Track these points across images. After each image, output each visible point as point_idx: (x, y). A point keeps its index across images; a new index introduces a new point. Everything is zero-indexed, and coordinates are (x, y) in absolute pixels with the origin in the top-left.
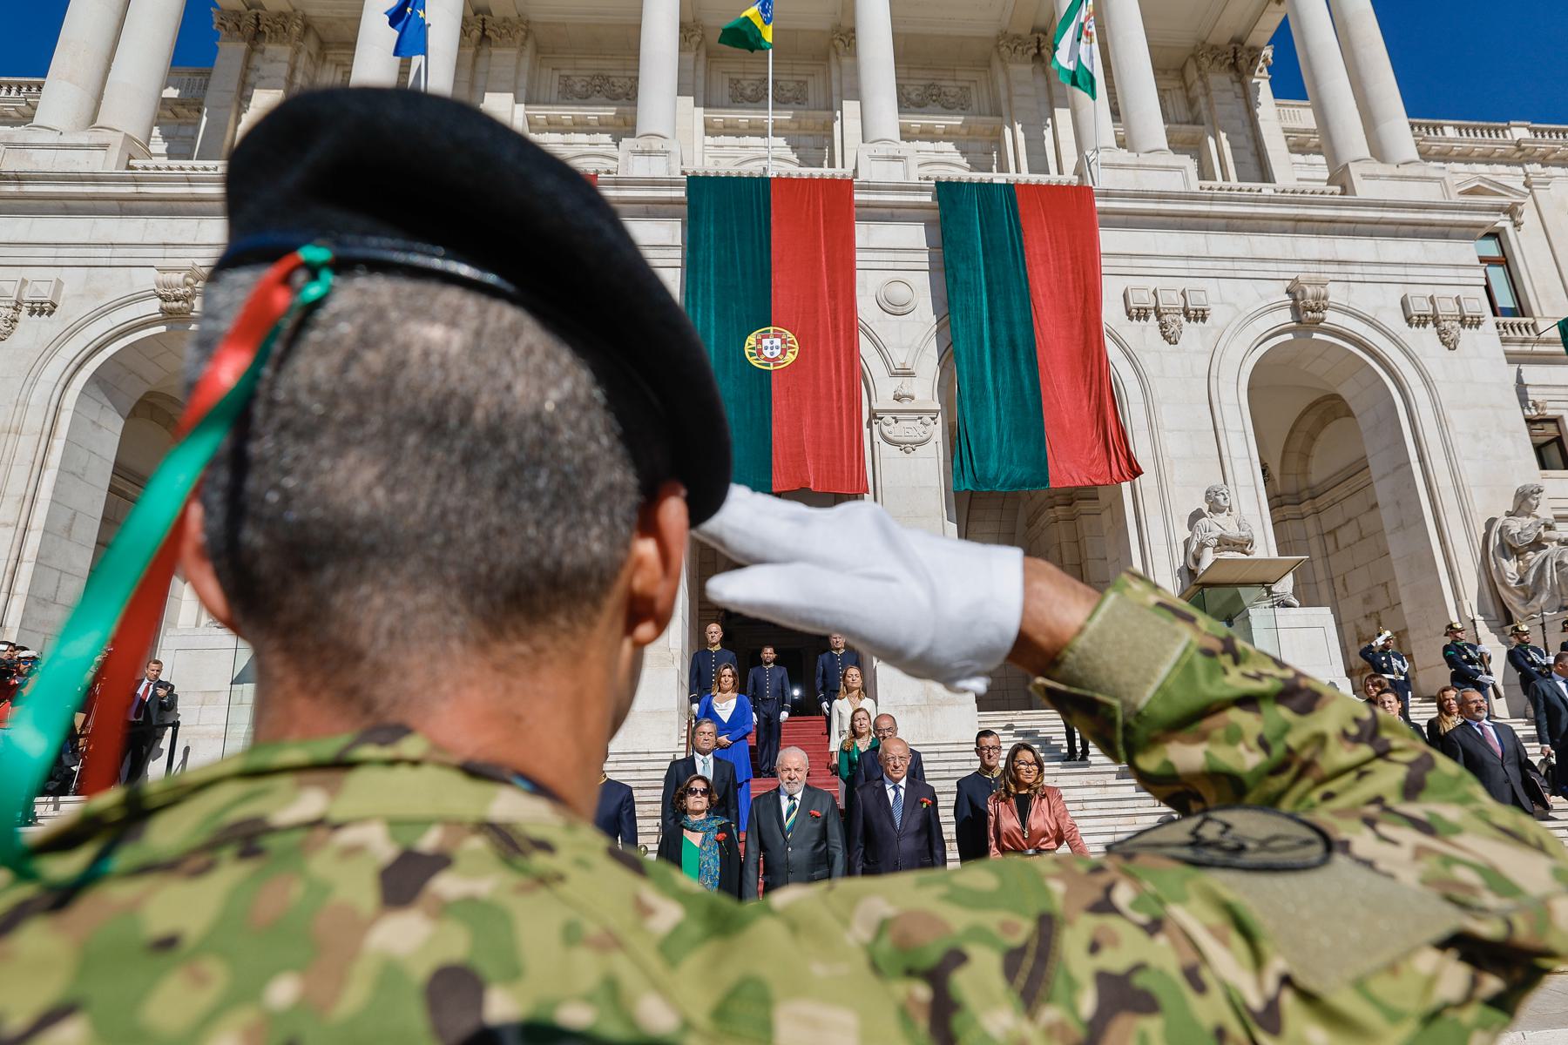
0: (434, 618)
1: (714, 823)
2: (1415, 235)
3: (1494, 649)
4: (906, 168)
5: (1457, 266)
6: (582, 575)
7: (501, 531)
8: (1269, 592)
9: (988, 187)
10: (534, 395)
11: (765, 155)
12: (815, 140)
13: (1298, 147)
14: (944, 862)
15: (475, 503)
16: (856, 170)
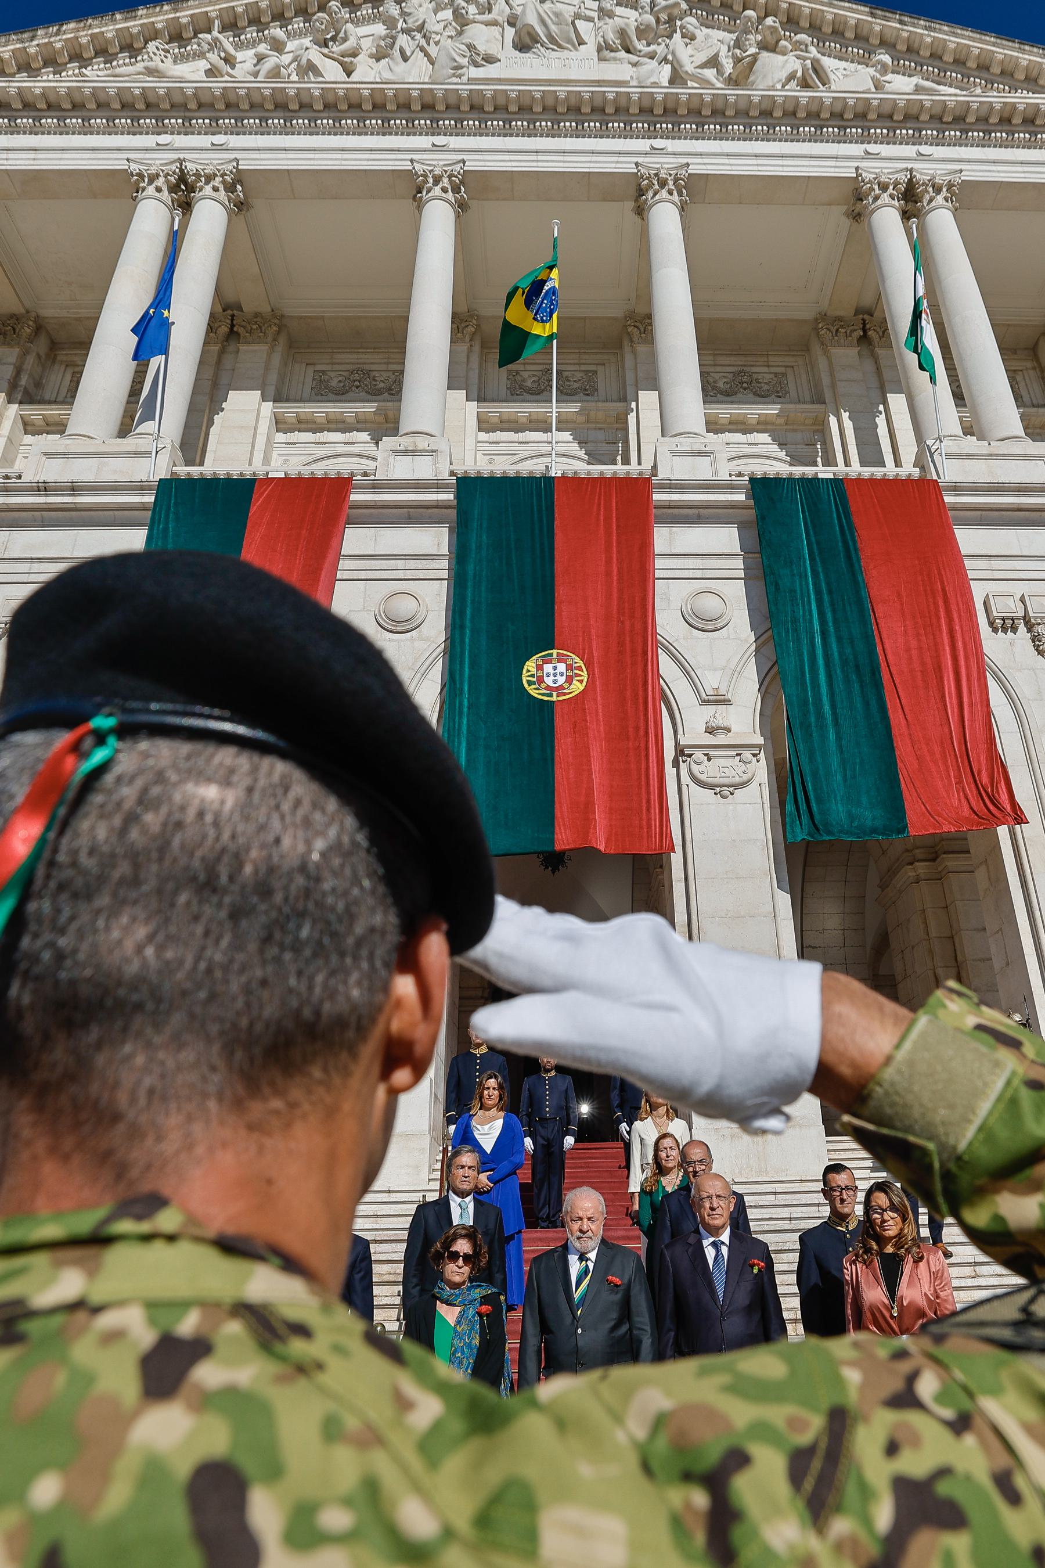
0: (193, 1077)
4: (714, 465)
6: (340, 1023)
7: (264, 983)
9: (811, 484)
10: (301, 848)
12: (607, 435)
15: (240, 957)
16: (655, 467)
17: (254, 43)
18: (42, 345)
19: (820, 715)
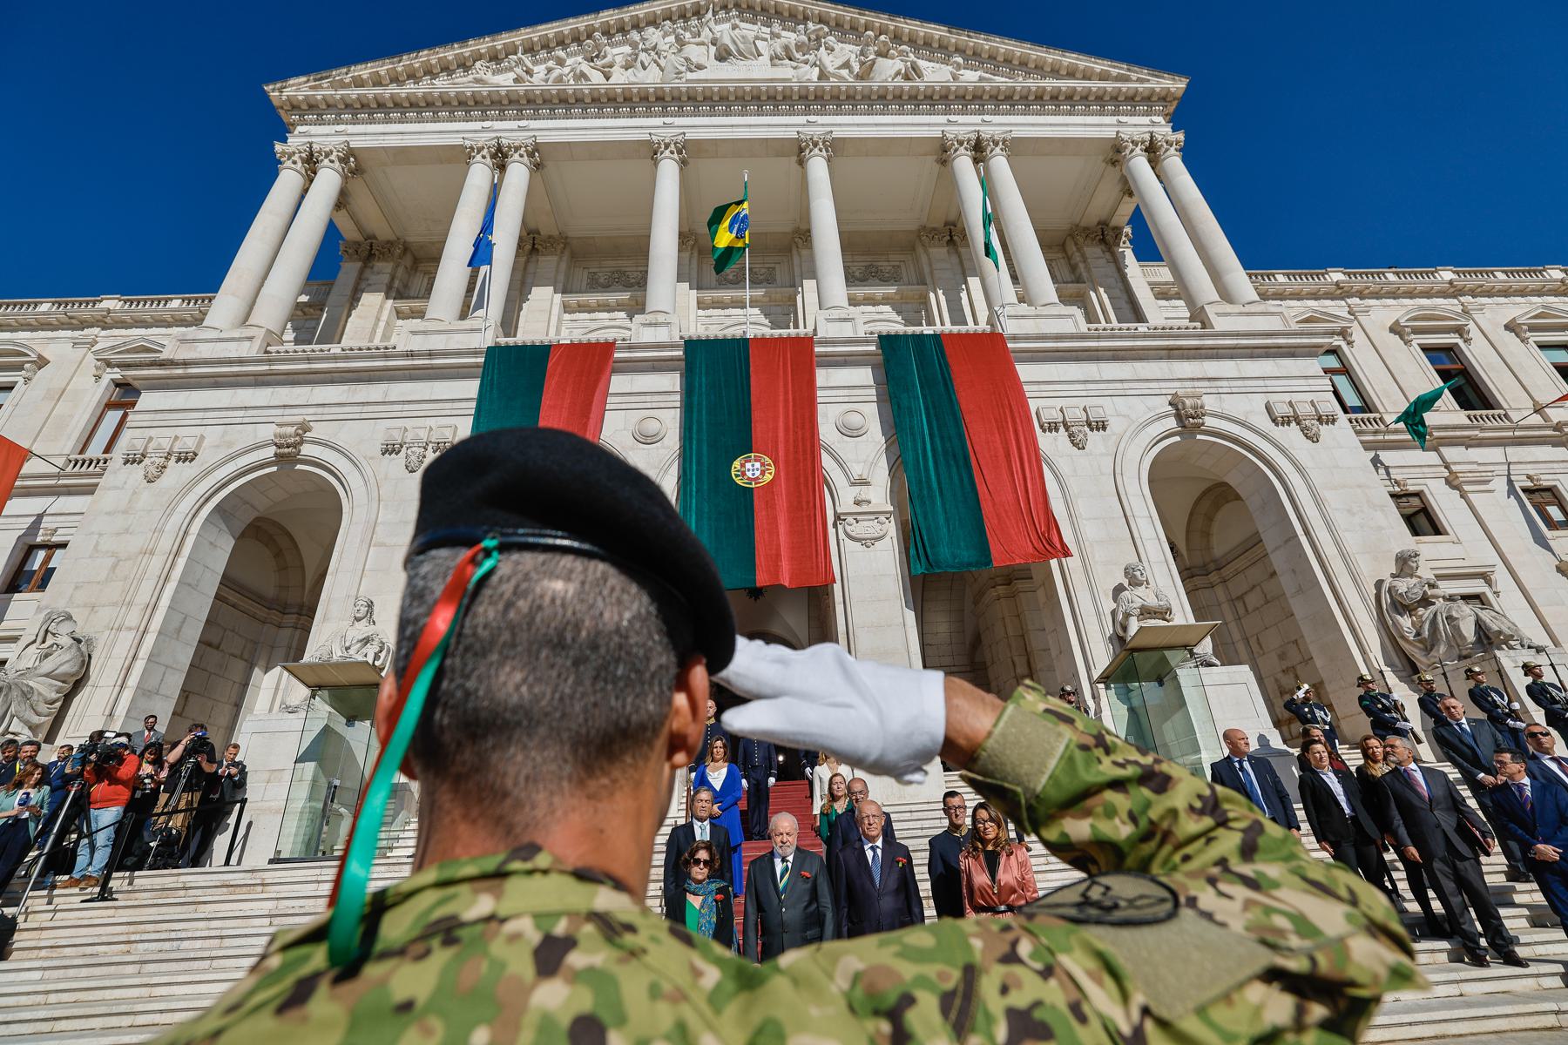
1: (713, 886)
2: (1268, 356)
3: (1405, 696)
5: (1306, 377)
8: (1192, 654)
9: (919, 338)
11: (745, 320)
12: (783, 310)
13: (1162, 294)
14: (923, 919)
17: (545, 61)
18: (408, 261)
19: (930, 488)
